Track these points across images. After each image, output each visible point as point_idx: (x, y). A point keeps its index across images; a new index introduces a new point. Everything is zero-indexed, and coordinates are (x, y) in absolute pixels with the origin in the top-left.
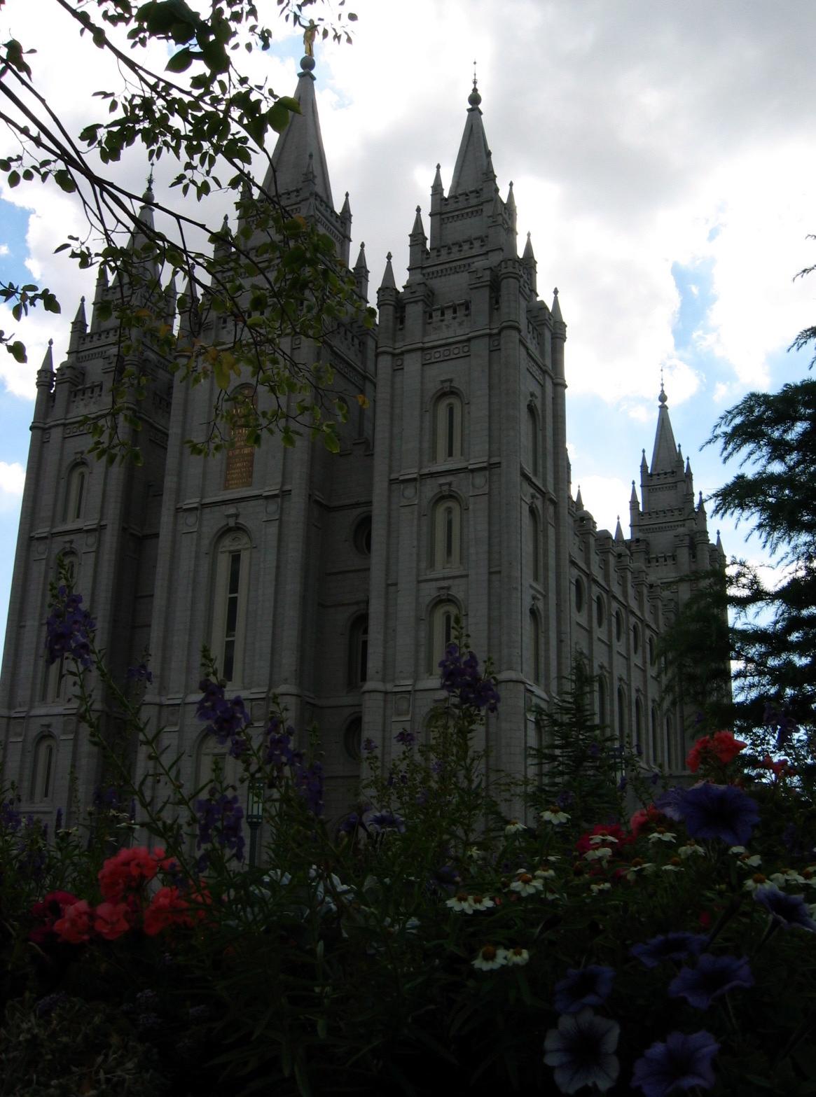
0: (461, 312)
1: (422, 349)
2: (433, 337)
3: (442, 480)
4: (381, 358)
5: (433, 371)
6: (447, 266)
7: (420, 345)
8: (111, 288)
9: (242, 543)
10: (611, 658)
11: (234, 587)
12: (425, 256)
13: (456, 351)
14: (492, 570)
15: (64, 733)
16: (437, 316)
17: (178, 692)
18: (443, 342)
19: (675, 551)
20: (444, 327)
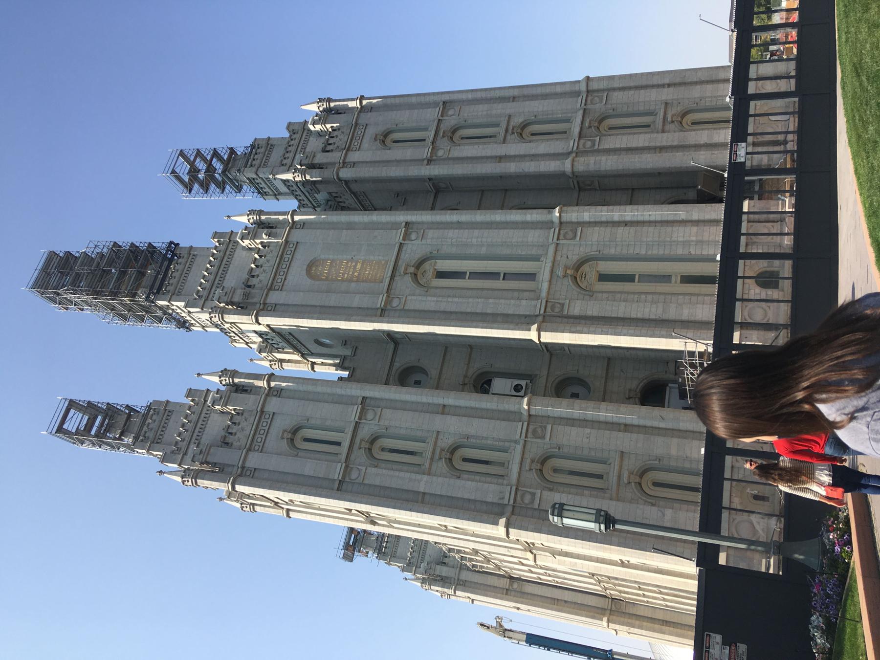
5: (365, 145)
15: (543, 437)
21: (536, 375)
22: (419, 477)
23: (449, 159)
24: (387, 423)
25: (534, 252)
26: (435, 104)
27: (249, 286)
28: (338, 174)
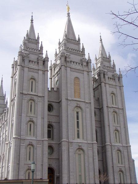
4: (102, 83)
5: (111, 88)
9: (79, 110)
11: (78, 118)
21: (53, 141)
22: (25, 114)
23: (108, 112)
24: (38, 104)
25: (85, 137)
26: (123, 106)
27: (71, 62)
28: (102, 82)
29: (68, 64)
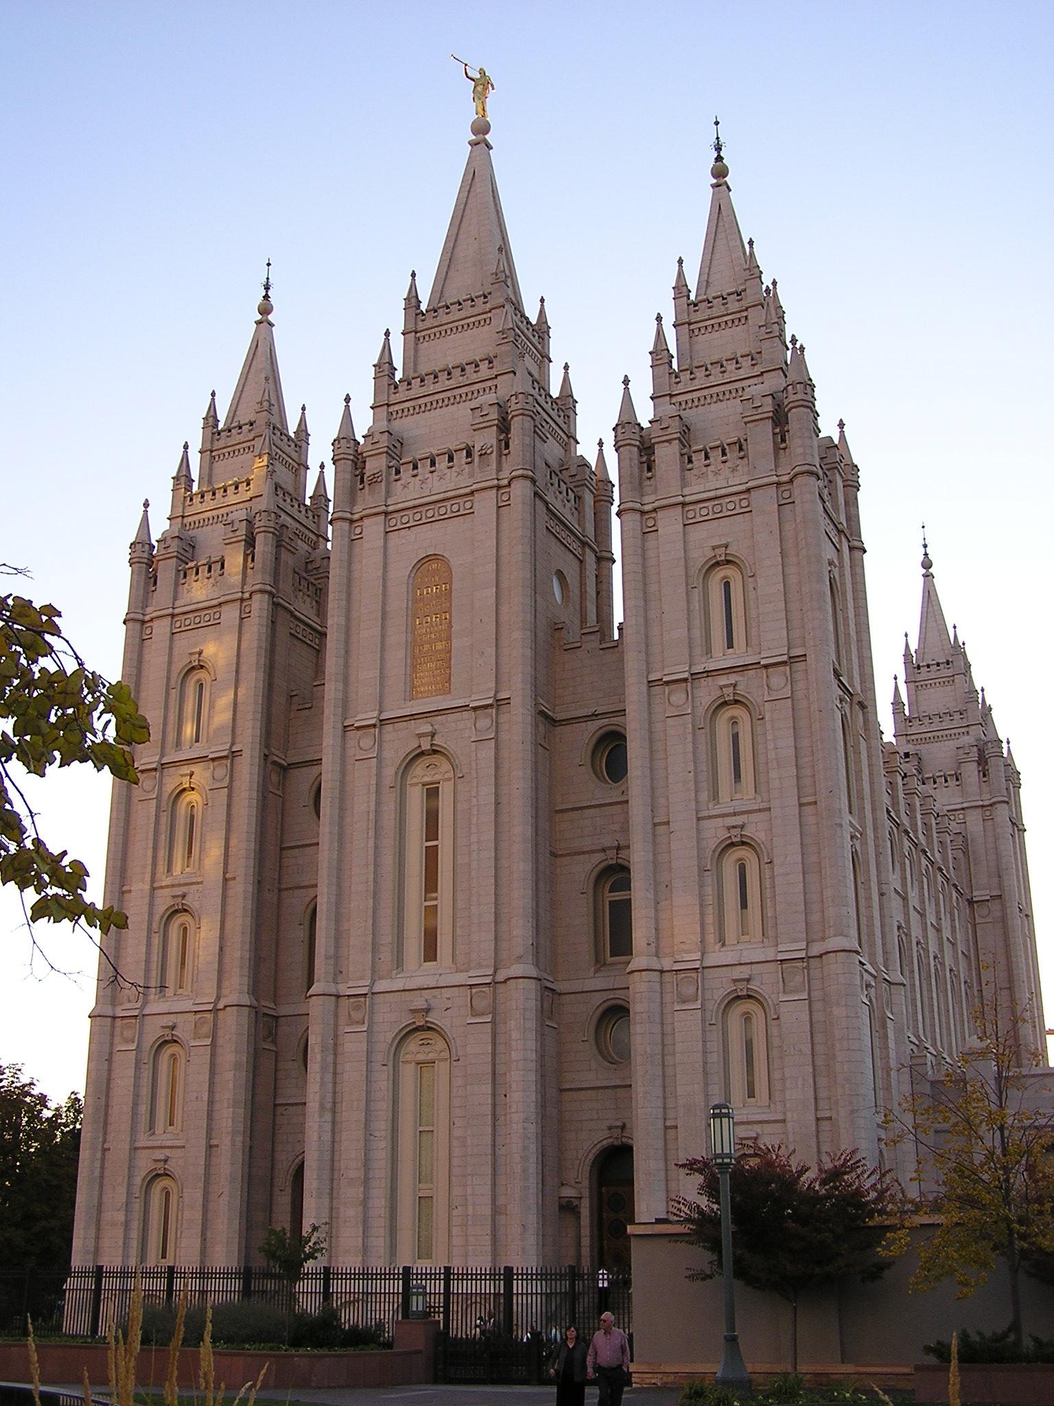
0: (732, 454)
1: (684, 504)
2: (696, 489)
3: (723, 681)
5: (697, 533)
6: (706, 392)
7: (681, 499)
8: (223, 431)
9: (439, 771)
10: (907, 914)
11: (432, 831)
12: (674, 380)
13: (731, 506)
14: (804, 800)
16: (698, 459)
17: (362, 978)
18: (712, 494)
19: (959, 768)
20: (711, 475)
22: (148, 878)
29: (369, 500)
